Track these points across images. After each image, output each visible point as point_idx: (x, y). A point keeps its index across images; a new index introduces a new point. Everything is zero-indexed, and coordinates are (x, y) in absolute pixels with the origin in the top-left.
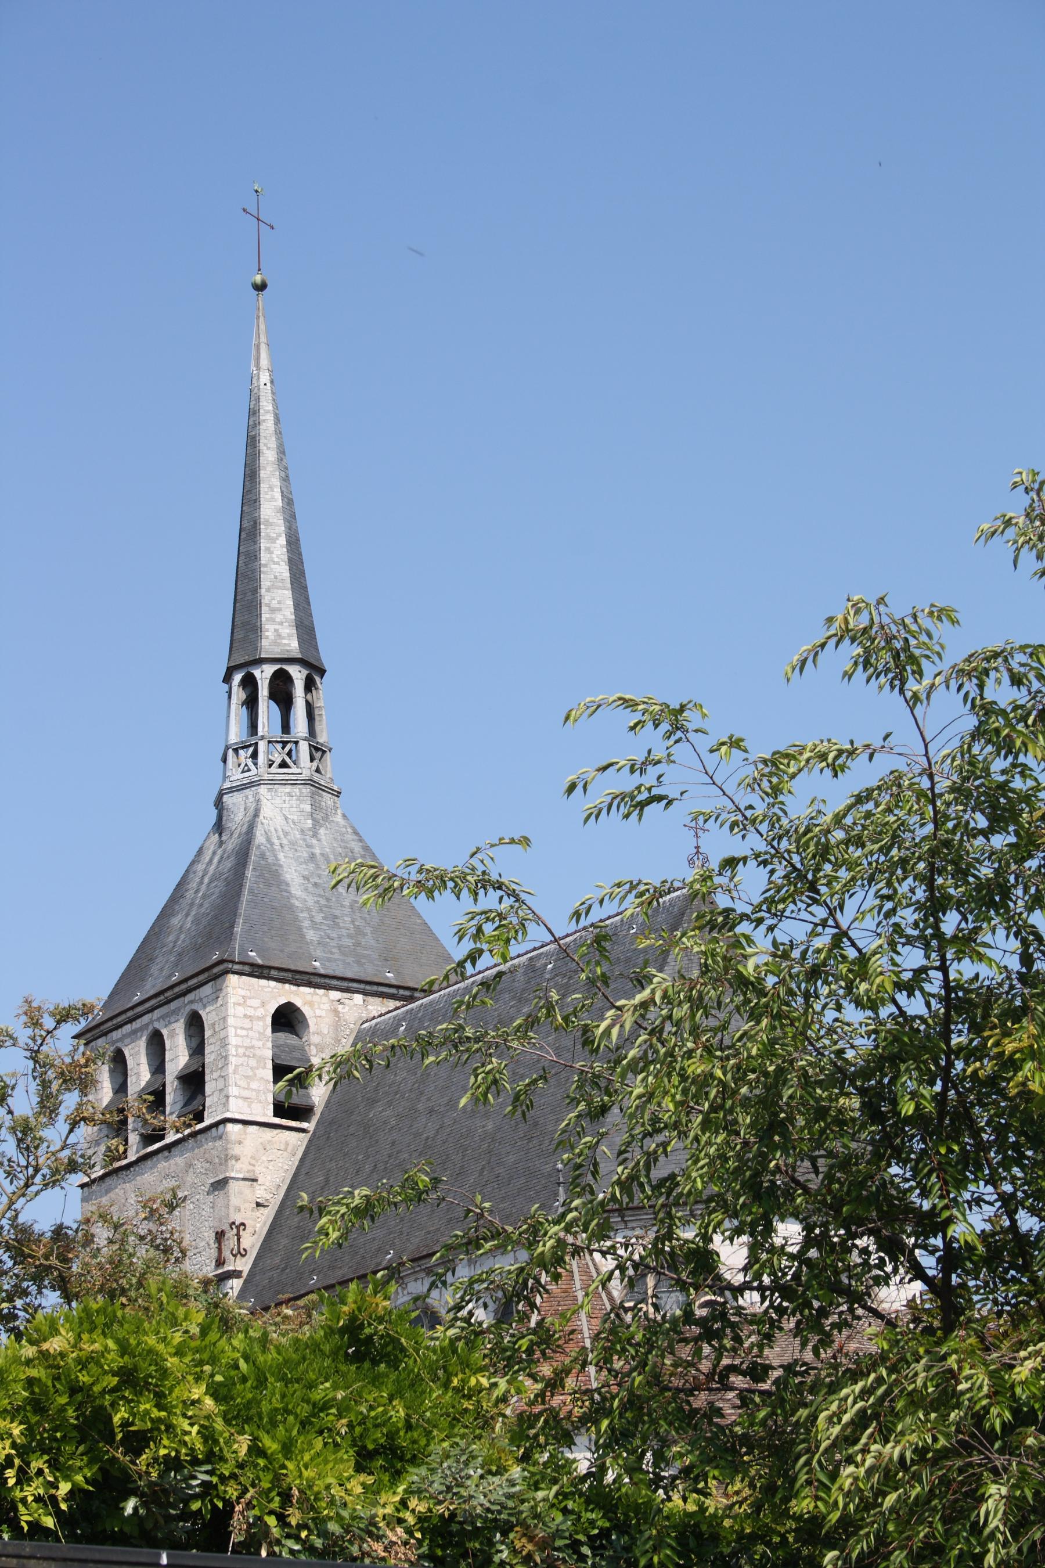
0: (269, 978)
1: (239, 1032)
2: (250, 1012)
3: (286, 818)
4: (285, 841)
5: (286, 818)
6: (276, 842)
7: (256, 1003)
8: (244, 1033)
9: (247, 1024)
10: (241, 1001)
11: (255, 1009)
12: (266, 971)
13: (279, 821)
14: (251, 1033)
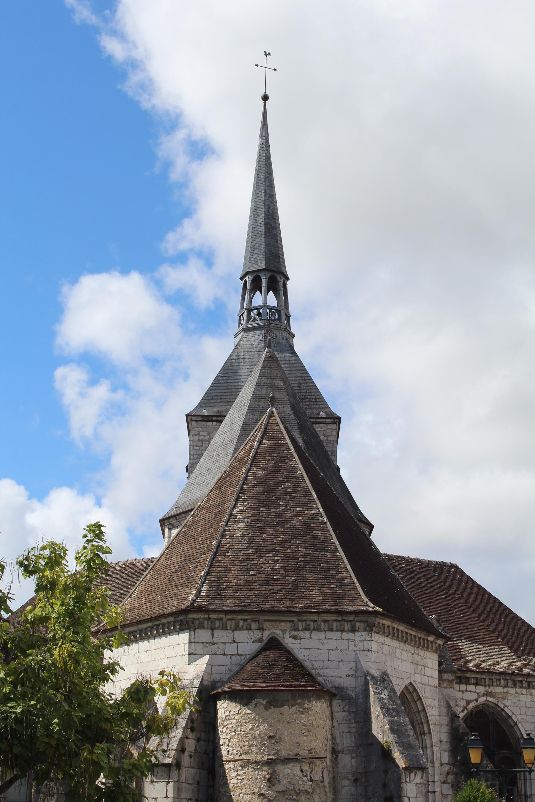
0: (213, 421)
1: (195, 448)
2: (201, 438)
3: (252, 345)
4: (247, 356)
5: (252, 345)
6: (242, 357)
7: (205, 433)
8: (198, 448)
9: (199, 443)
10: (197, 433)
11: (204, 436)
12: (210, 418)
13: (249, 346)
14: (201, 448)
